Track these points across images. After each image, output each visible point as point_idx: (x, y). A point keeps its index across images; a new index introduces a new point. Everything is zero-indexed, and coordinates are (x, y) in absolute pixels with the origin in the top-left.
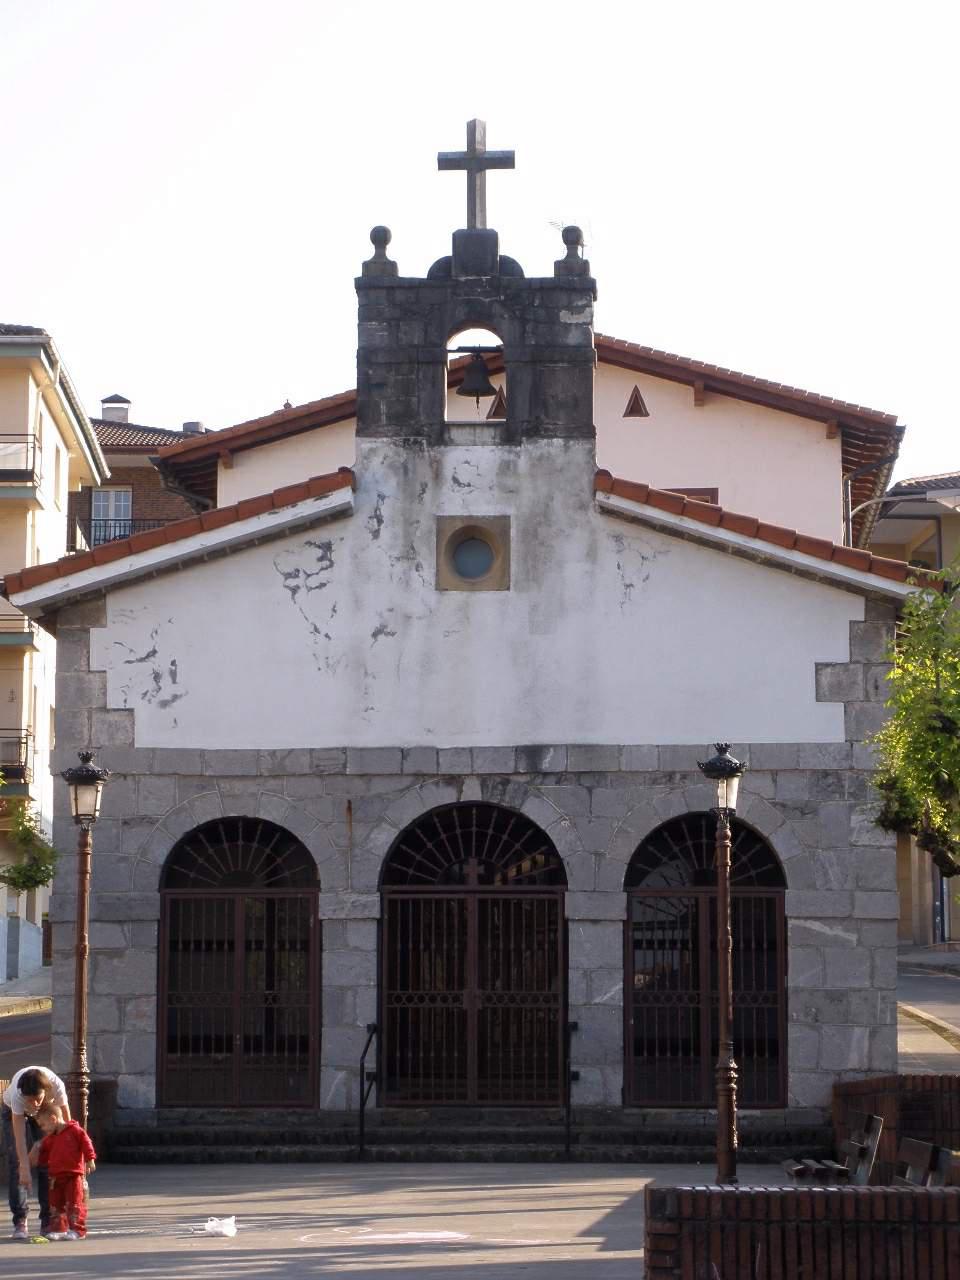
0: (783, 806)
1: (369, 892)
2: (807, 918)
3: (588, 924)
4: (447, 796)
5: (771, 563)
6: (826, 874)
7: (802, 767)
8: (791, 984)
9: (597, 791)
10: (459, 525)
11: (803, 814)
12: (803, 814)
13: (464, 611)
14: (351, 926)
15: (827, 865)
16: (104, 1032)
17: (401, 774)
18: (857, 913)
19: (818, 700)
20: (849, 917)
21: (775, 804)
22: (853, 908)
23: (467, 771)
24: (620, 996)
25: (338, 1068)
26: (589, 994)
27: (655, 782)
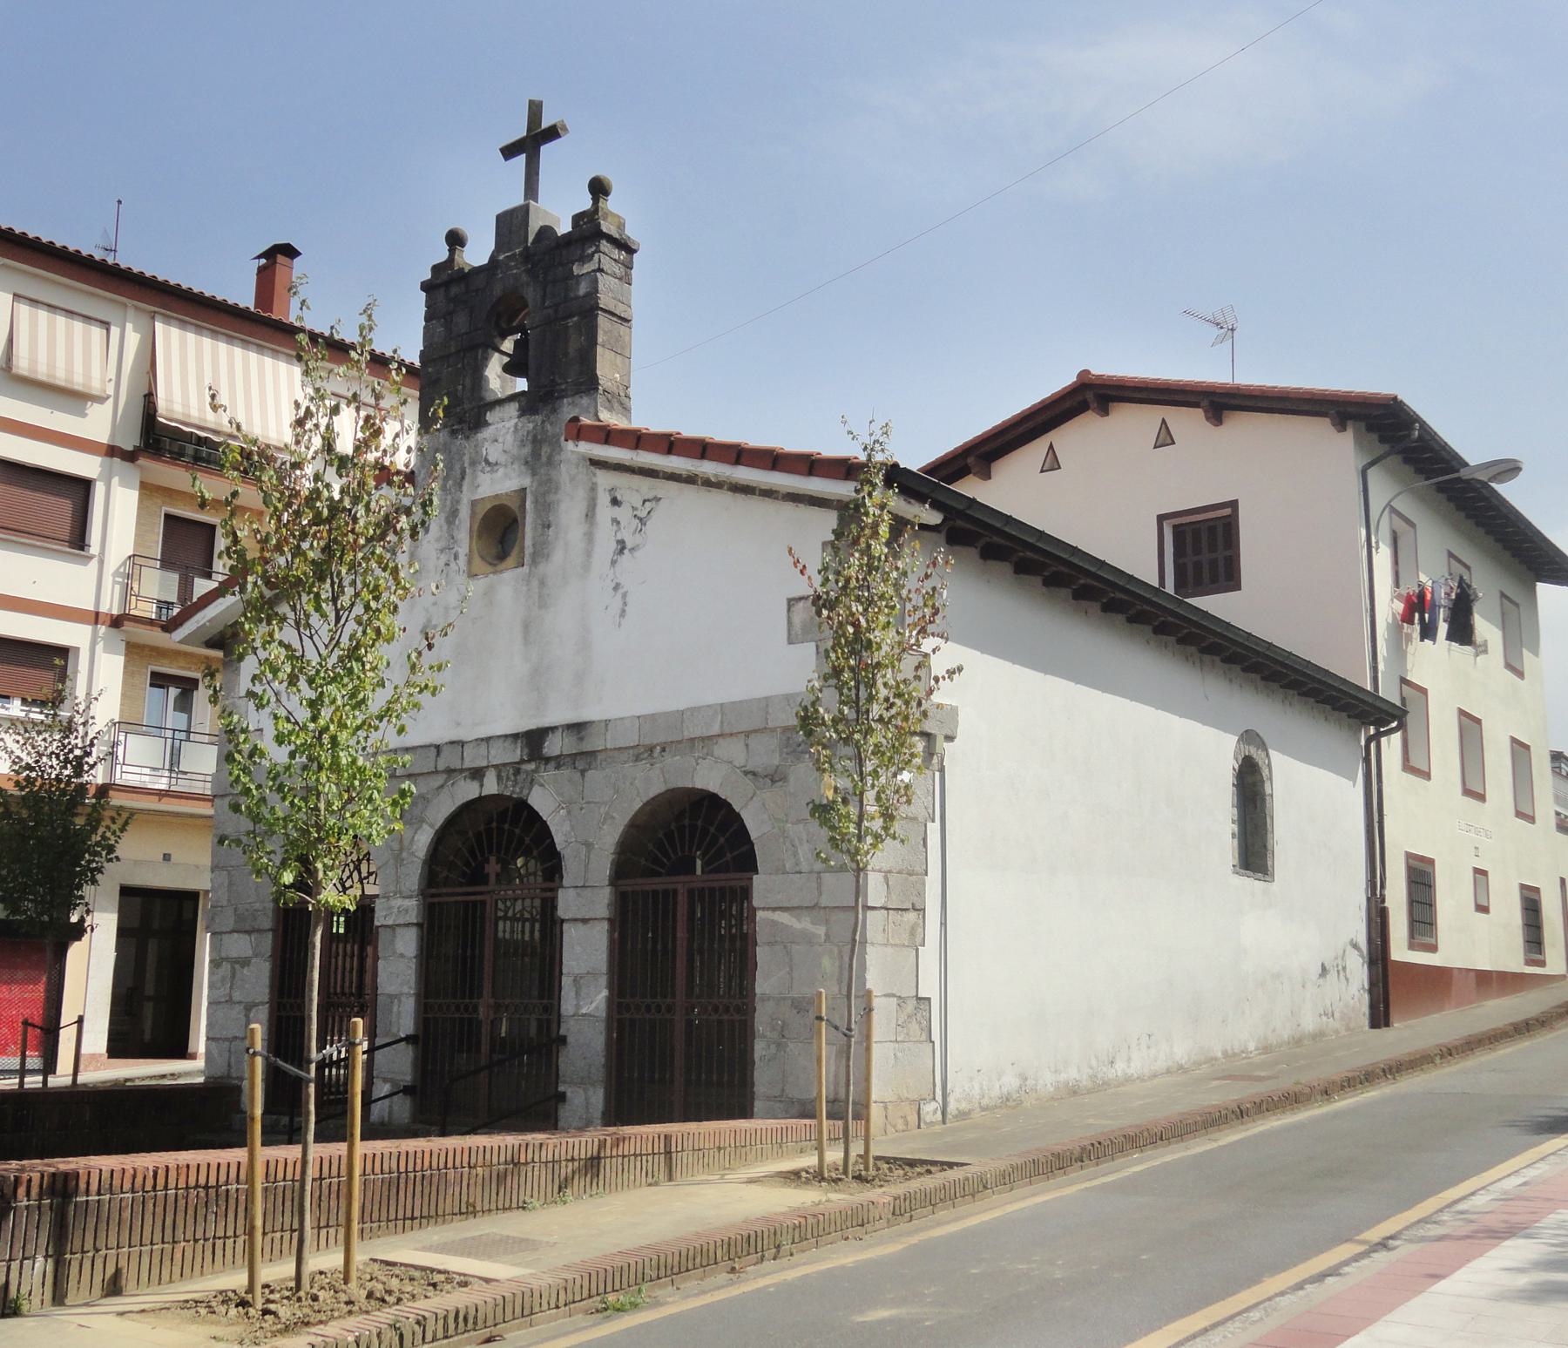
0: (754, 774)
1: (411, 897)
2: (775, 909)
3: (580, 924)
4: (468, 791)
5: (795, 498)
6: (795, 854)
7: (770, 725)
8: (758, 990)
9: (589, 774)
10: (489, 506)
11: (773, 782)
12: (773, 782)
13: (489, 593)
14: (399, 930)
15: (797, 842)
16: (236, 1038)
17: (436, 772)
18: (824, 902)
19: (790, 642)
20: (815, 907)
21: (746, 773)
22: (820, 894)
23: (484, 764)
24: (603, 1006)
25: (385, 1080)
26: (578, 1006)
27: (637, 758)
